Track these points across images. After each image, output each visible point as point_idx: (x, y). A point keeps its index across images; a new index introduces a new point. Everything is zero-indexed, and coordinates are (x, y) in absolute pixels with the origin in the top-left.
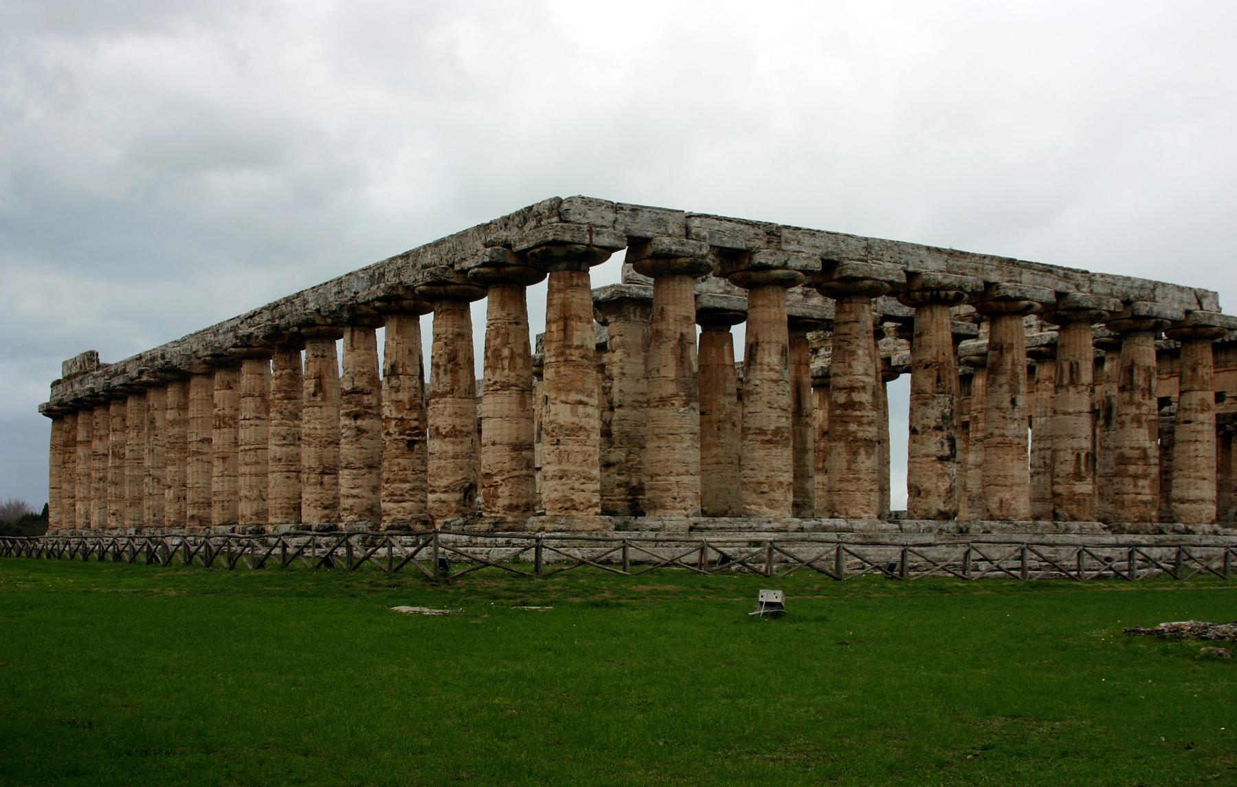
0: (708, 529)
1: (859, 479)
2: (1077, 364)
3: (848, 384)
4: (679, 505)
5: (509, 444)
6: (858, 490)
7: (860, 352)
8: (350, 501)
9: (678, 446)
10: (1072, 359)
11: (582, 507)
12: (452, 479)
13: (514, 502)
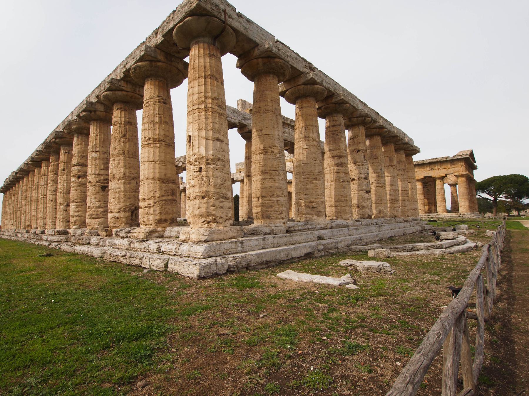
0: (295, 230)
1: (347, 200)
3: (339, 154)
4: (279, 216)
5: (159, 179)
6: (347, 206)
8: (75, 219)
9: (277, 178)
11: (221, 221)
12: (122, 205)
13: (163, 217)
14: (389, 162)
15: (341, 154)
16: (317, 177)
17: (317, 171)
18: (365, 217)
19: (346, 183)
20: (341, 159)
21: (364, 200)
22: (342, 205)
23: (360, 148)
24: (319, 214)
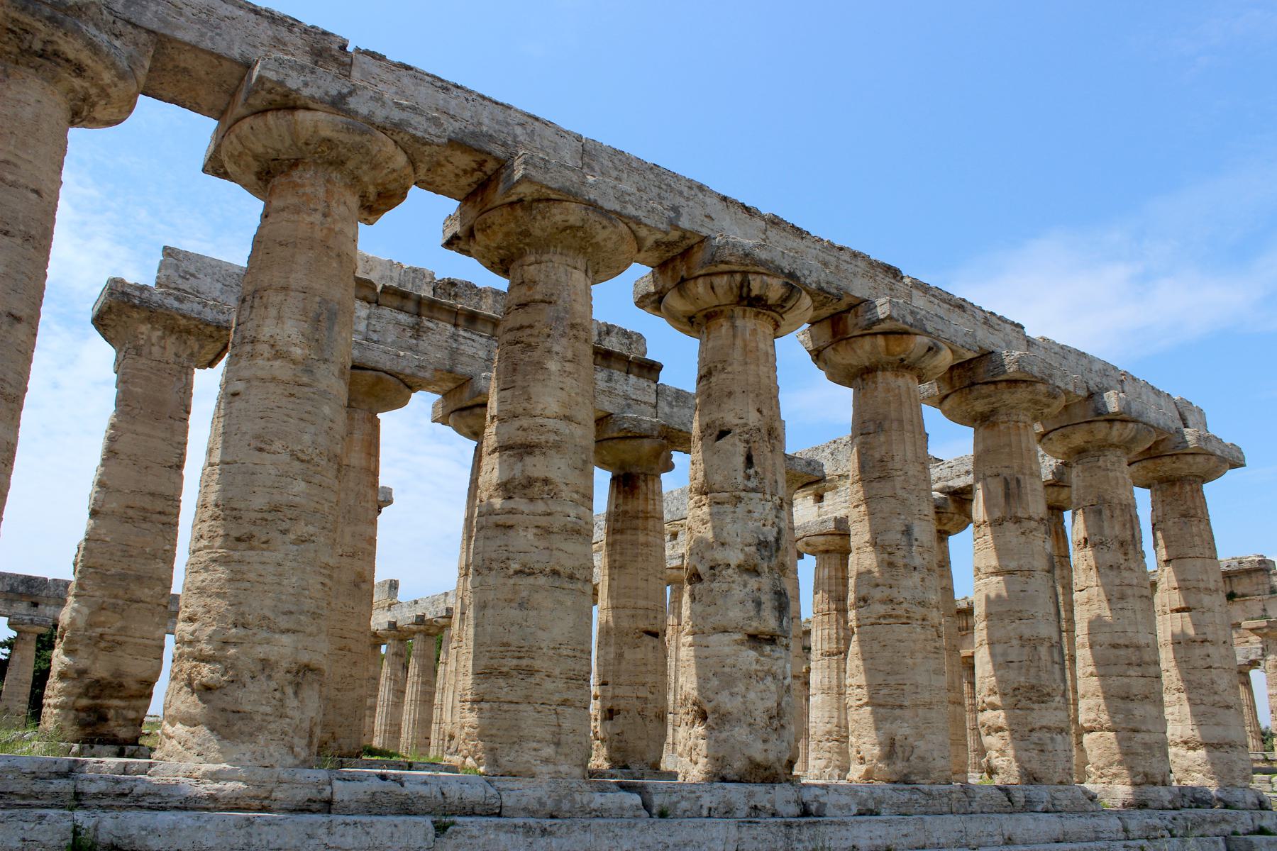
1: (531, 672)
2: (1018, 481)
3: (519, 437)
6: (528, 700)
7: (553, 366)
10: (1006, 472)
14: (1002, 500)
15: (533, 438)
16: (255, 530)
17: (259, 501)
18: (729, 772)
19: (542, 580)
20: (529, 460)
21: (728, 682)
22: (505, 693)
23: (730, 419)
24: (229, 724)
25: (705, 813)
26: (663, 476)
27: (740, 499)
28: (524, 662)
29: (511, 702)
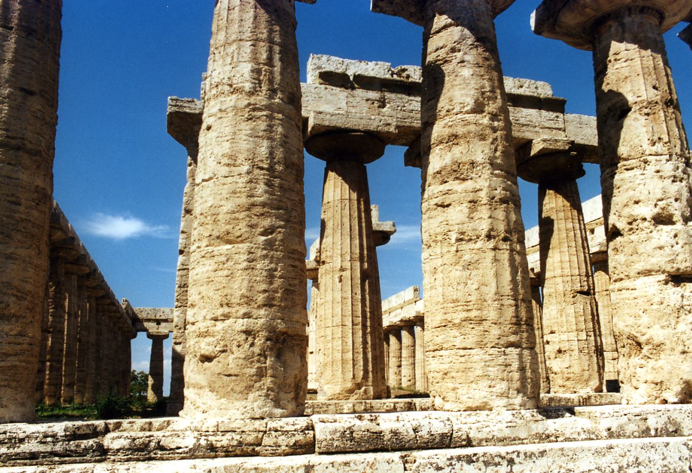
6: (481, 345)
25: (653, 432)
26: (578, 181)
27: (646, 162)
28: (473, 314)
29: (465, 349)
